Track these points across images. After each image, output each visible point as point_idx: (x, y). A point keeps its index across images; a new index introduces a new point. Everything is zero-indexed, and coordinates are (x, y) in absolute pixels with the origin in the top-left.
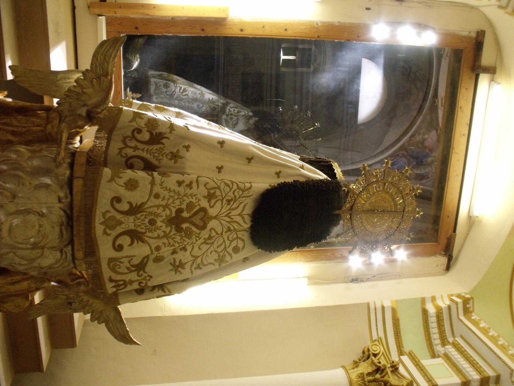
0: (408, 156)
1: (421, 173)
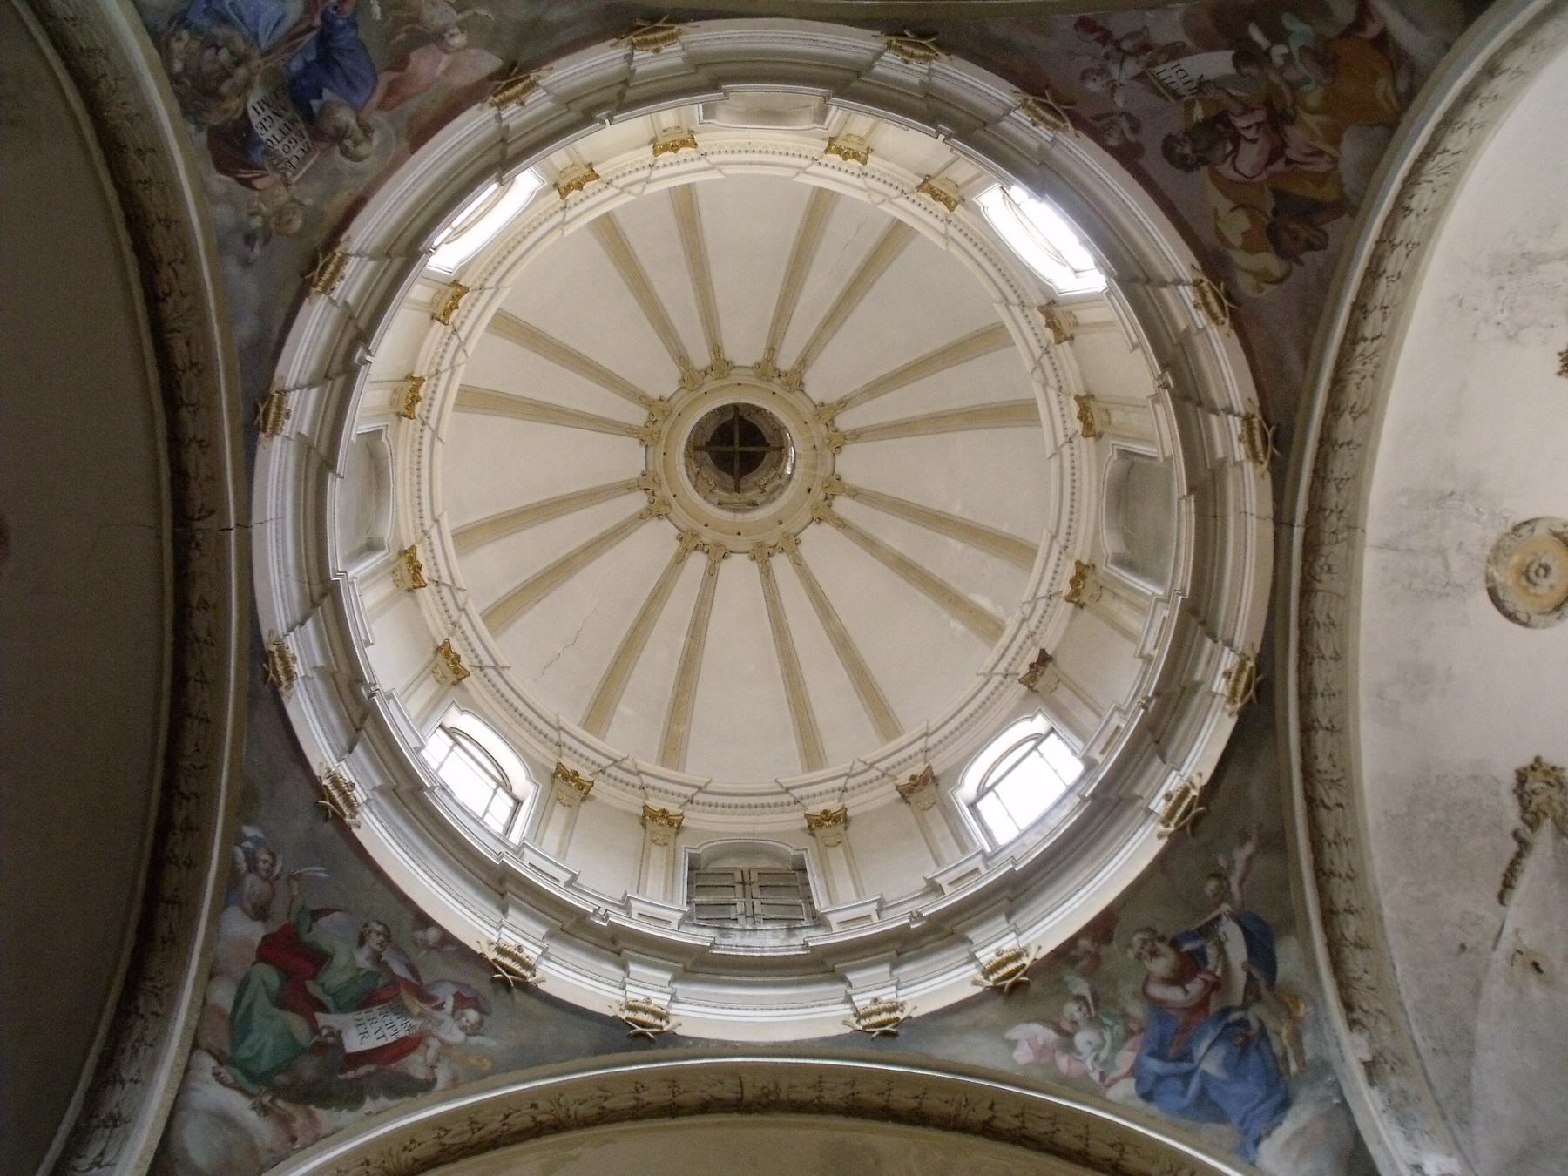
0: (324, 17)
1: (259, 131)
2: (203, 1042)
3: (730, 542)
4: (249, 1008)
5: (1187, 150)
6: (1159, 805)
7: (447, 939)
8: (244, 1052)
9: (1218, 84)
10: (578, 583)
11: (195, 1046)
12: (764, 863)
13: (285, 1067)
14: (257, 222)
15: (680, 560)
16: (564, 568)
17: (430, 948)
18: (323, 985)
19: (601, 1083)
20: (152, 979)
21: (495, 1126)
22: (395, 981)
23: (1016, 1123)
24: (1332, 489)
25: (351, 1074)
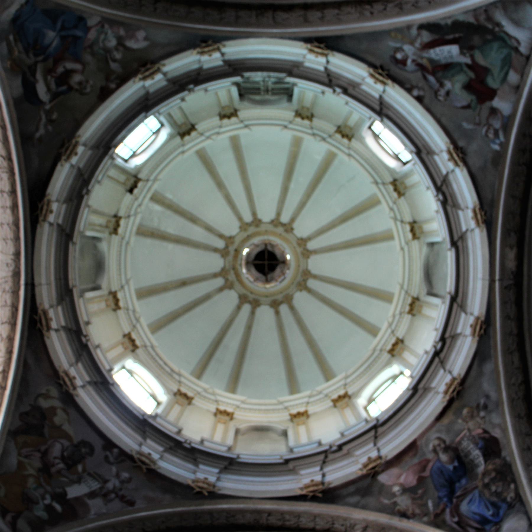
3: (271, 228)
4: (502, 68)
5: (83, 450)
6: (80, 149)
7: (409, 90)
8: (505, 51)
9: (72, 482)
10: (338, 211)
12: (257, 98)
13: (486, 42)
14: (482, 414)
15: (293, 220)
16: (344, 218)
19: (339, 21)
22: (433, 74)
24: (9, 302)
25: (457, 35)
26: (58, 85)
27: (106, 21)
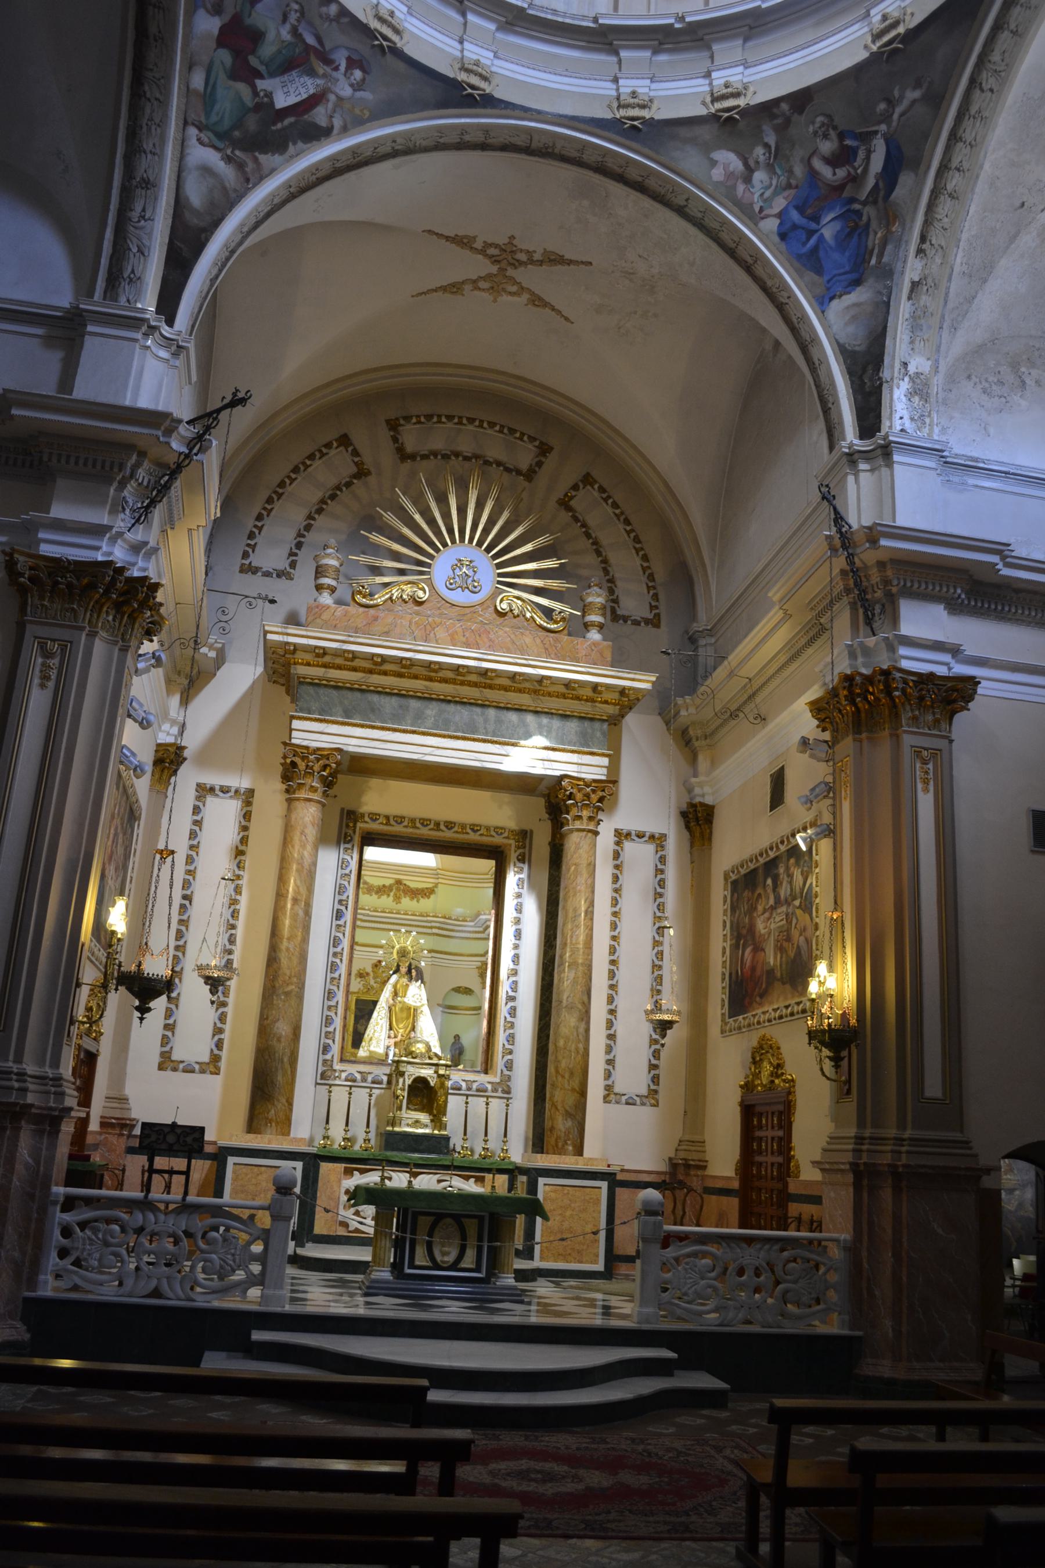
2: (190, 120)
4: (215, 83)
8: (214, 118)
11: (186, 123)
13: (239, 124)
17: (331, 20)
18: (259, 58)
19: (440, 129)
20: (152, 70)
21: (369, 153)
22: (308, 47)
23: (700, 215)
25: (279, 126)
26: (854, 151)
27: (754, 217)
